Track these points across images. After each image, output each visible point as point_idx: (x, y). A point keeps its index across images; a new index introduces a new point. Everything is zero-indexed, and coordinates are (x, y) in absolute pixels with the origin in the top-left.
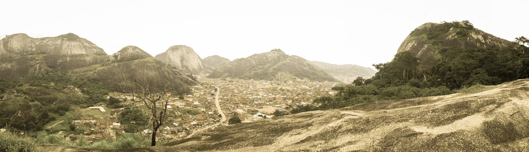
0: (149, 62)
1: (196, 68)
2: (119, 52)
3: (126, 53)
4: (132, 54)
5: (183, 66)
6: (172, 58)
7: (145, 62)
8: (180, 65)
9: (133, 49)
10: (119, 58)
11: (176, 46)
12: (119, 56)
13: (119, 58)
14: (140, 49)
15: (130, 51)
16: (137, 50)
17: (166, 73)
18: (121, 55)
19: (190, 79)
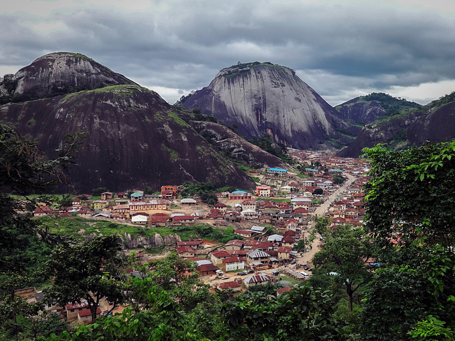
0: (110, 96)
1: (305, 129)
2: (22, 70)
3: (45, 73)
4: (63, 76)
5: (264, 126)
6: (228, 104)
7: (101, 96)
8: (254, 121)
9: (69, 62)
10: (19, 90)
11: (240, 66)
12: (21, 82)
13: (19, 90)
14: (93, 63)
15: (60, 67)
16: (82, 64)
17: (166, 127)
18: (27, 79)
19: (255, 148)
